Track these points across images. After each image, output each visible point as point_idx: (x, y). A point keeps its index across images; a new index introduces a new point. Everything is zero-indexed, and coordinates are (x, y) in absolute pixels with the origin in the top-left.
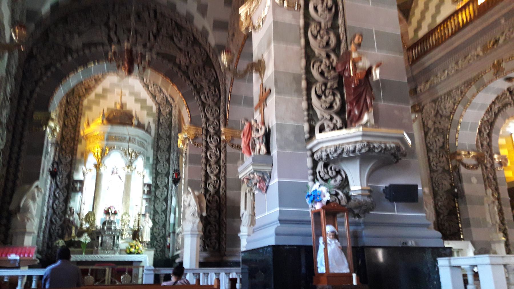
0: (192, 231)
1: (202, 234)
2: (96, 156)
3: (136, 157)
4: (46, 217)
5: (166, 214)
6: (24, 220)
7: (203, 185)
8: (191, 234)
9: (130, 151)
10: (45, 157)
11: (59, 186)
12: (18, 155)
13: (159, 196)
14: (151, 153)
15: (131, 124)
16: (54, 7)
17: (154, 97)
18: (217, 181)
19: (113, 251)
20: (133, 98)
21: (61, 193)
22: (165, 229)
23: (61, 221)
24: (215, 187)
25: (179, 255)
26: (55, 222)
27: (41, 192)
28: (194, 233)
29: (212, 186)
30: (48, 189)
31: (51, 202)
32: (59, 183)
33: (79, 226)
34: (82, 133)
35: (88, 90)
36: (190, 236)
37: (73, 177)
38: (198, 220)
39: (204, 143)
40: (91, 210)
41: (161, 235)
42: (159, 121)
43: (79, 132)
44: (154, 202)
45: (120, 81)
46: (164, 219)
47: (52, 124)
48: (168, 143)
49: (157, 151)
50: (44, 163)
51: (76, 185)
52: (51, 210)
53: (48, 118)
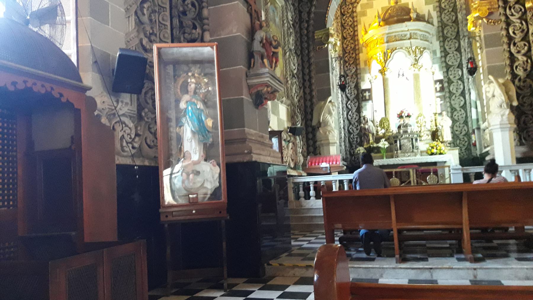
0: (501, 124)
1: (515, 126)
2: (379, 61)
3: (421, 53)
4: (344, 128)
5: (466, 110)
6: (326, 133)
7: (508, 70)
8: (501, 128)
9: (414, 48)
10: (332, 73)
11: (351, 99)
12: (310, 76)
13: (454, 91)
14: (436, 45)
15: (409, 19)
18: (527, 61)
19: (414, 154)
21: (352, 104)
22: (467, 126)
23: (357, 130)
24: (525, 70)
25: (489, 152)
26: (352, 132)
27: (335, 106)
28: (504, 126)
29: (521, 68)
30: (340, 102)
31: (345, 113)
32: (349, 95)
33: (375, 133)
34: (361, 42)
36: (500, 130)
37: (360, 87)
38: (508, 111)
39: (503, 18)
41: (464, 133)
42: (440, 6)
43: (358, 40)
44: (450, 98)
46: (464, 115)
47: (331, 40)
48: (455, 28)
49: (444, 41)
50: (333, 79)
51: (365, 94)
52: (346, 121)
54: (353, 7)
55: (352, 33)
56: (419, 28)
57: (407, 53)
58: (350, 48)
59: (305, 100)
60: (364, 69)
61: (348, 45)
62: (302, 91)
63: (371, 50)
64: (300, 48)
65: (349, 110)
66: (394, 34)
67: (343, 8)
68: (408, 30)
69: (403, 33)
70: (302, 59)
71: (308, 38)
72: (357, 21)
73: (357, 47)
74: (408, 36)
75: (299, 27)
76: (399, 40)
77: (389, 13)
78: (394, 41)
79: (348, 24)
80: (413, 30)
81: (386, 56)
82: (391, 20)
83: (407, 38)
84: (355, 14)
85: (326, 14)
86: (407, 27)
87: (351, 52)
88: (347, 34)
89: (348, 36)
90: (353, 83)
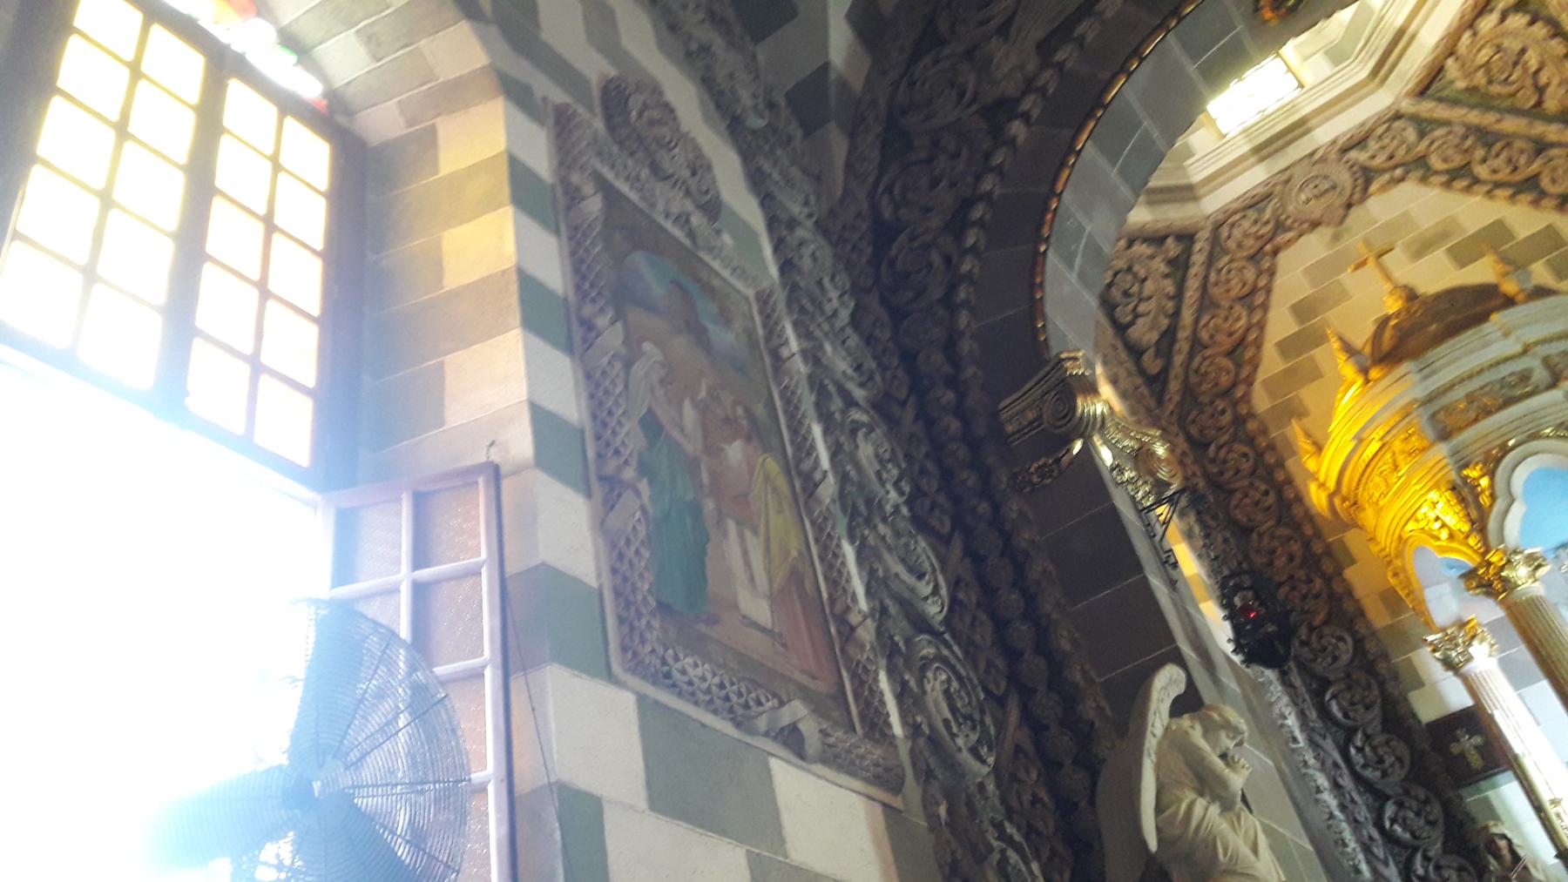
2: (1444, 534)
11: (1389, 791)
16: (867, 23)
20: (1439, 255)
21: (1411, 815)
27: (1234, 731)
30: (1337, 813)
32: (1370, 774)
34: (1317, 498)
35: (1243, 350)
37: (1414, 715)
43: (1299, 499)
45: (1336, 238)
51: (1455, 749)
54: (1235, 404)
55: (1271, 499)
59: (1051, 765)
61: (1273, 552)
62: (1014, 715)
63: (1379, 511)
65: (1403, 852)
66: (1459, 393)
68: (1525, 351)
69: (1505, 370)
72: (1272, 447)
73: (1318, 548)
74: (1540, 375)
75: (917, 418)
78: (1476, 420)
79: (1238, 471)
81: (1470, 499)
84: (1252, 426)
85: (1034, 320)
87: (1301, 574)
89: (1260, 517)
90: (1368, 707)
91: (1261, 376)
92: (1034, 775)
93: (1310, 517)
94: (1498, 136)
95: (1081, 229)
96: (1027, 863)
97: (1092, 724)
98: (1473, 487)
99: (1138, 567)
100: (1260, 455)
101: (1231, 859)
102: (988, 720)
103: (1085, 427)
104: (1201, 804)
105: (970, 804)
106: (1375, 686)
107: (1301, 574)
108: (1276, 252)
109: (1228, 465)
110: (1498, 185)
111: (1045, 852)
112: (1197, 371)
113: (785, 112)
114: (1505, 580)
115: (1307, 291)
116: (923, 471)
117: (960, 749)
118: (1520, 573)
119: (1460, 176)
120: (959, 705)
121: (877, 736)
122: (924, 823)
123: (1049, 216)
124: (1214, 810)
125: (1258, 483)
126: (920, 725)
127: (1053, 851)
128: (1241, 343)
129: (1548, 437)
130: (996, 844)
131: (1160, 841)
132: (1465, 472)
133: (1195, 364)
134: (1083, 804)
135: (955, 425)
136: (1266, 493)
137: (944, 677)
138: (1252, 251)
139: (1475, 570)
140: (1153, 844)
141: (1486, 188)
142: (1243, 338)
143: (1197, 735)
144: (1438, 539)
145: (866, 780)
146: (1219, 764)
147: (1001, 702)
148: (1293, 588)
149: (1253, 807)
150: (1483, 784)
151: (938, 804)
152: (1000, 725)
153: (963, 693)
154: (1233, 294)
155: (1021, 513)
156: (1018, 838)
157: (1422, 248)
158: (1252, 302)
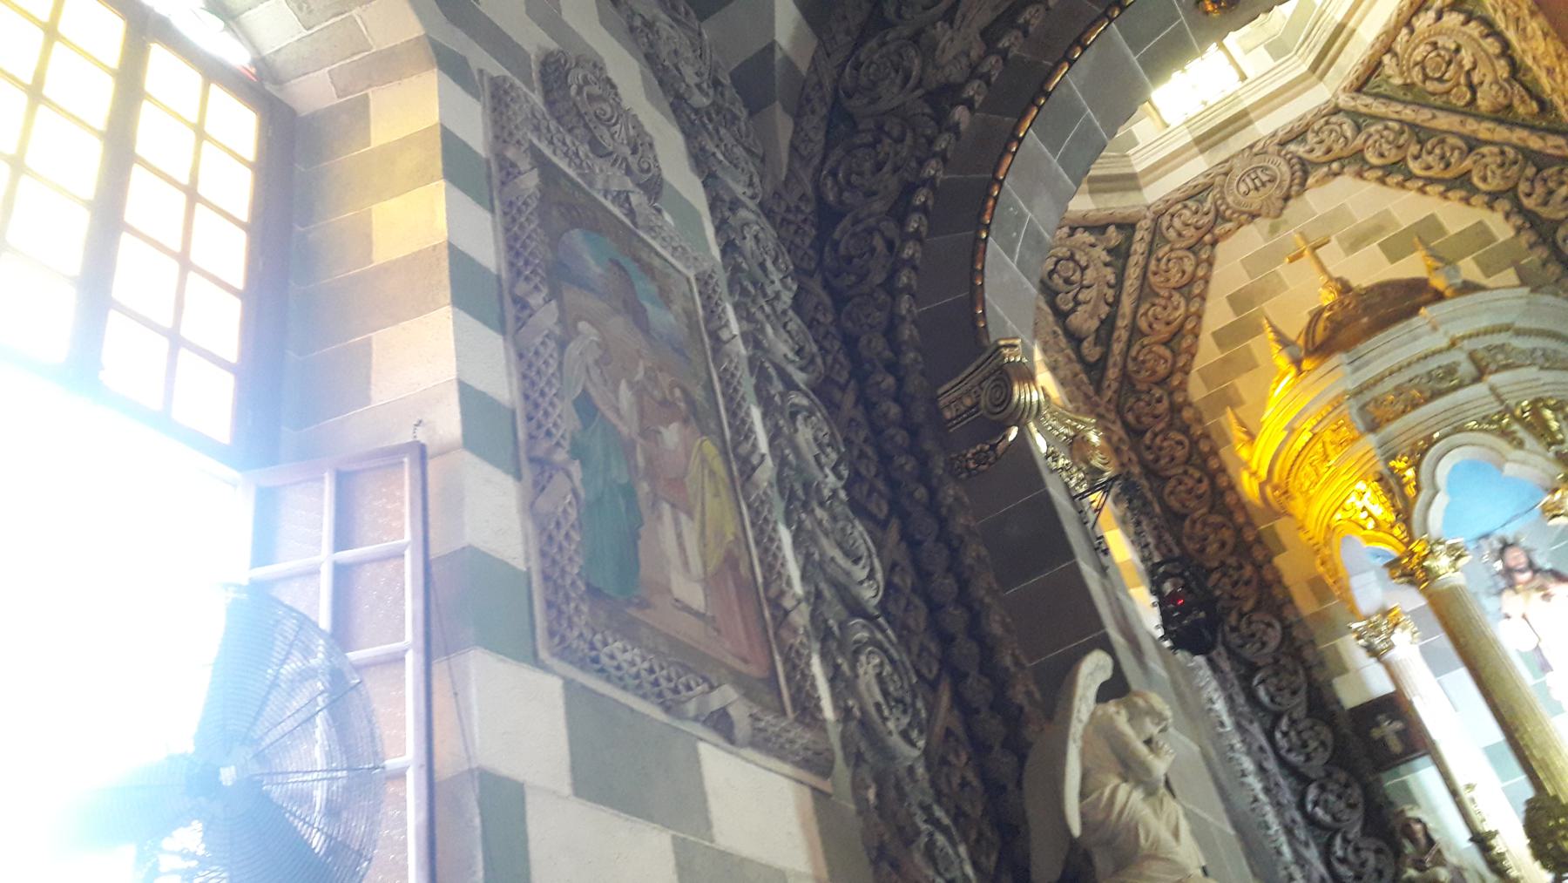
2: (1370, 524)
11: (1313, 776)
12: (970, 608)
17: (1461, 184)
20: (1374, 247)
21: (1332, 798)
27: (1159, 717)
30: (1262, 796)
31: (1312, 854)
32: (1293, 758)
34: (1249, 486)
35: (1180, 339)
37: (1338, 702)
40: (1530, 793)
43: (1232, 487)
45: (1274, 230)
51: (1376, 733)
53: (1009, 375)
54: (1171, 394)
55: (1204, 486)
56: (1505, 320)
57: (1502, 444)
58: (1215, 546)
59: (979, 747)
60: (1321, 618)
62: (945, 699)
63: (1309, 501)
64: (880, 485)
65: (1324, 834)
66: (1389, 384)
67: (1130, 409)
68: (1453, 344)
69: (1432, 364)
70: (905, 536)
71: (914, 432)
72: (1206, 436)
73: (1249, 536)
74: (1466, 369)
76: (1427, 401)
77: (1328, 318)
78: (1404, 412)
79: (1173, 459)
80: (1478, 335)
81: (1396, 489)
82: (1343, 336)
83: (1467, 381)
84: (1187, 414)
85: (973, 306)
86: (1442, 330)
88: (1184, 495)
89: (1192, 504)
90: (1294, 693)
91: (1199, 363)
92: (964, 758)
93: (1241, 505)
94: (1432, 132)
95: (1021, 216)
96: (954, 845)
97: (1021, 709)
98: (1399, 479)
99: (1068, 553)
100: (1194, 443)
101: (1152, 845)
102: (920, 704)
103: (1020, 415)
104: (1124, 789)
105: (898, 787)
106: (1301, 672)
107: (1232, 561)
108: (1214, 243)
109: (1163, 452)
110: (1430, 181)
111: (973, 836)
112: (1135, 359)
113: (730, 92)
114: (1427, 570)
115: (1241, 282)
116: (862, 455)
117: (890, 733)
118: (1441, 563)
119: (1394, 172)
120: (891, 689)
121: (808, 720)
122: (852, 807)
123: (991, 203)
124: (1138, 795)
125: (1191, 470)
126: (852, 708)
127: (981, 834)
128: (1178, 333)
129: (1472, 430)
130: (924, 827)
131: (1084, 824)
132: (1392, 463)
133: (1133, 352)
134: (1011, 787)
135: (894, 410)
136: (1200, 481)
137: (877, 661)
138: (1192, 241)
139: (1398, 560)
140: (1076, 829)
141: (1420, 183)
142: (1182, 326)
143: (1122, 721)
144: (1364, 529)
145: (797, 764)
146: (1143, 750)
147: (933, 686)
148: (1224, 575)
149: (1177, 792)
150: (1402, 768)
151: (867, 788)
152: (931, 709)
153: (896, 677)
154: (1173, 283)
155: (957, 499)
156: (946, 821)
157: (1355, 242)
158: (1190, 293)
